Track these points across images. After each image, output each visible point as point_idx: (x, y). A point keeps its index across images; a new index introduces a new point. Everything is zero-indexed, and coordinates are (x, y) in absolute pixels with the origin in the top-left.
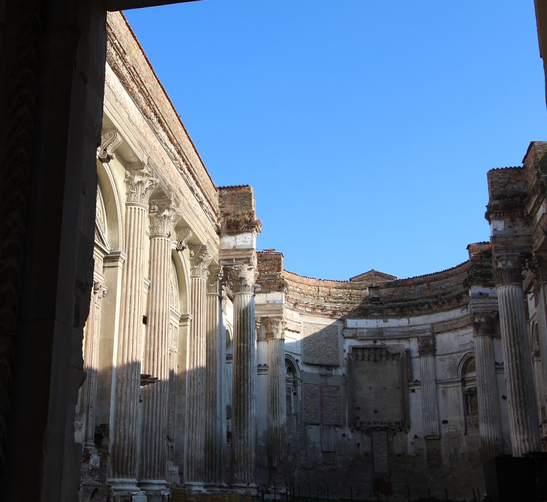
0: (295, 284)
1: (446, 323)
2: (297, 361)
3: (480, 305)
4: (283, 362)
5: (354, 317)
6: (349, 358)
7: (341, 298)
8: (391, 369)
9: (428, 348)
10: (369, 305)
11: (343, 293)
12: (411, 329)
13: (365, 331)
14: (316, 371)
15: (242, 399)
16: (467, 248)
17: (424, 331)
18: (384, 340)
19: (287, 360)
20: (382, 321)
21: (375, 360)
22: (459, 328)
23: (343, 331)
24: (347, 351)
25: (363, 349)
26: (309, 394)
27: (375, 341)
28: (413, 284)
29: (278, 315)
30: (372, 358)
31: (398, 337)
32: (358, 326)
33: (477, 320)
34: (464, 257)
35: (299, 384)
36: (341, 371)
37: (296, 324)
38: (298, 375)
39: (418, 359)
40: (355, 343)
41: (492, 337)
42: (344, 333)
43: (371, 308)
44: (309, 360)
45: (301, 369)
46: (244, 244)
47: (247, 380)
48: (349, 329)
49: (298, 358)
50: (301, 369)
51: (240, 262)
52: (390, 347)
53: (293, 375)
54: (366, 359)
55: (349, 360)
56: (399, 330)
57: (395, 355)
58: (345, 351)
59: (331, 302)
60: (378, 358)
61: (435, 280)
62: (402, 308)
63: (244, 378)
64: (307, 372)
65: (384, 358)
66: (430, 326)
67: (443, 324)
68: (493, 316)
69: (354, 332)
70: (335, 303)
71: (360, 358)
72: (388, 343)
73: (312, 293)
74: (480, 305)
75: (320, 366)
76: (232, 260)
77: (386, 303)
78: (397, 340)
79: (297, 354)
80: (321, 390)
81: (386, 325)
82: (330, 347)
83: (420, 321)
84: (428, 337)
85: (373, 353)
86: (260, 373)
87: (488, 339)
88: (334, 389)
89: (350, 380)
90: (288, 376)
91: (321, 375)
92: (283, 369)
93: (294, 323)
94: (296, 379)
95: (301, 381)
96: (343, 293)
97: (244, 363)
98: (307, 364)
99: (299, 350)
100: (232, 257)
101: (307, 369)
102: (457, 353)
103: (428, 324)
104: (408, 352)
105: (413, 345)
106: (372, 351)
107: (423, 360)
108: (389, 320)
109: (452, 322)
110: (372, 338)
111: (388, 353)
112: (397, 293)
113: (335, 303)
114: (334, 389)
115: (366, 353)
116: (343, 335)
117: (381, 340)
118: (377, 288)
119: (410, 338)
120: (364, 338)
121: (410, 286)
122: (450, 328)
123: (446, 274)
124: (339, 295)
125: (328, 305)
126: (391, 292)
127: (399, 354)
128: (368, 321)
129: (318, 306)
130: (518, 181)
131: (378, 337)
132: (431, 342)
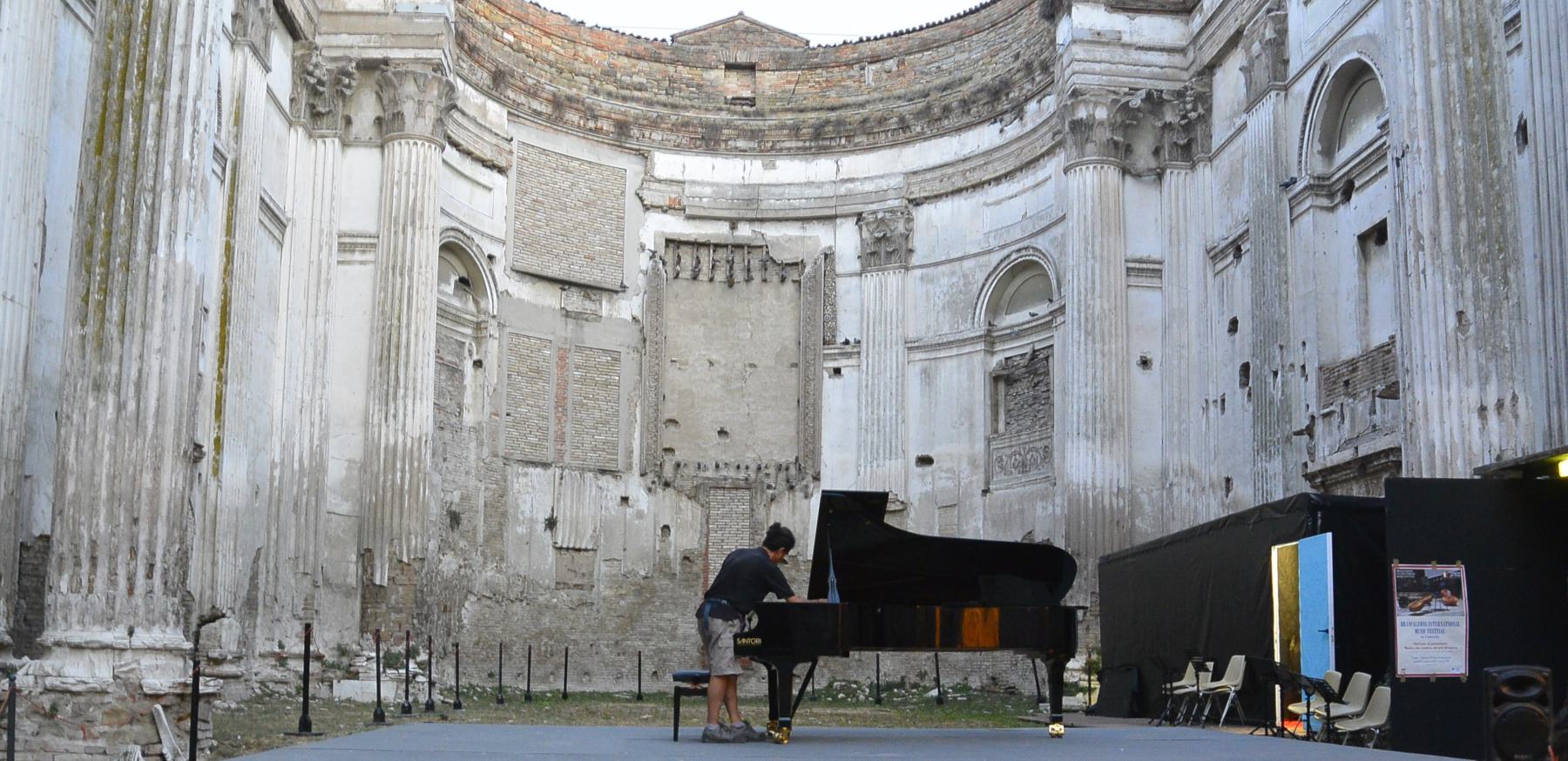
1: (950, 170)
2: (491, 257)
3: (1097, 67)
5: (678, 148)
6: (655, 268)
7: (640, 88)
8: (772, 312)
9: (887, 248)
10: (724, 116)
11: (649, 75)
12: (843, 190)
13: (708, 190)
14: (551, 298)
15: (126, 178)
17: (881, 195)
18: (762, 220)
20: (758, 163)
21: (730, 282)
23: (641, 188)
24: (650, 246)
25: (696, 245)
26: (524, 369)
27: (733, 227)
28: (859, 61)
29: (424, 54)
30: (721, 276)
31: (802, 214)
32: (687, 178)
33: (1082, 113)
35: (493, 329)
36: (629, 307)
37: (494, 140)
38: (491, 304)
39: (855, 280)
40: (678, 227)
41: (1125, 172)
42: (645, 194)
43: (728, 125)
45: (501, 288)
48: (660, 181)
49: (497, 251)
50: (501, 288)
52: (777, 242)
53: (476, 302)
54: (703, 277)
55: (653, 276)
56: (808, 192)
57: (788, 269)
58: (643, 248)
59: (609, 94)
60: (739, 276)
61: (925, 47)
62: (818, 132)
63: (143, 75)
64: (520, 301)
66: (900, 179)
67: (938, 173)
68: (1136, 102)
70: (625, 99)
72: (771, 232)
73: (551, 57)
74: (1097, 67)
75: (564, 284)
77: (773, 111)
78: (799, 224)
79: (492, 238)
80: (562, 358)
81: (770, 177)
82: (597, 232)
83: (873, 169)
84: (892, 211)
85: (725, 257)
86: (348, 257)
87: (1112, 174)
88: (603, 359)
89: (649, 335)
90: (456, 303)
91: (567, 314)
93: (487, 137)
94: (482, 317)
95: (501, 326)
96: (649, 75)
98: (524, 274)
99: (499, 227)
101: (524, 291)
102: (975, 255)
104: (828, 256)
105: (846, 241)
106: (722, 254)
107: (871, 281)
108: (778, 163)
109: (968, 165)
110: (726, 214)
111: (768, 262)
112: (808, 88)
113: (625, 99)
114: (603, 359)
115: (706, 257)
116: (641, 199)
117: (751, 220)
118: (751, 68)
121: (849, 65)
122: (960, 183)
123: (958, 27)
124: (636, 79)
125: (604, 104)
126: (789, 82)
127: (798, 265)
129: (569, 99)
131: (743, 214)
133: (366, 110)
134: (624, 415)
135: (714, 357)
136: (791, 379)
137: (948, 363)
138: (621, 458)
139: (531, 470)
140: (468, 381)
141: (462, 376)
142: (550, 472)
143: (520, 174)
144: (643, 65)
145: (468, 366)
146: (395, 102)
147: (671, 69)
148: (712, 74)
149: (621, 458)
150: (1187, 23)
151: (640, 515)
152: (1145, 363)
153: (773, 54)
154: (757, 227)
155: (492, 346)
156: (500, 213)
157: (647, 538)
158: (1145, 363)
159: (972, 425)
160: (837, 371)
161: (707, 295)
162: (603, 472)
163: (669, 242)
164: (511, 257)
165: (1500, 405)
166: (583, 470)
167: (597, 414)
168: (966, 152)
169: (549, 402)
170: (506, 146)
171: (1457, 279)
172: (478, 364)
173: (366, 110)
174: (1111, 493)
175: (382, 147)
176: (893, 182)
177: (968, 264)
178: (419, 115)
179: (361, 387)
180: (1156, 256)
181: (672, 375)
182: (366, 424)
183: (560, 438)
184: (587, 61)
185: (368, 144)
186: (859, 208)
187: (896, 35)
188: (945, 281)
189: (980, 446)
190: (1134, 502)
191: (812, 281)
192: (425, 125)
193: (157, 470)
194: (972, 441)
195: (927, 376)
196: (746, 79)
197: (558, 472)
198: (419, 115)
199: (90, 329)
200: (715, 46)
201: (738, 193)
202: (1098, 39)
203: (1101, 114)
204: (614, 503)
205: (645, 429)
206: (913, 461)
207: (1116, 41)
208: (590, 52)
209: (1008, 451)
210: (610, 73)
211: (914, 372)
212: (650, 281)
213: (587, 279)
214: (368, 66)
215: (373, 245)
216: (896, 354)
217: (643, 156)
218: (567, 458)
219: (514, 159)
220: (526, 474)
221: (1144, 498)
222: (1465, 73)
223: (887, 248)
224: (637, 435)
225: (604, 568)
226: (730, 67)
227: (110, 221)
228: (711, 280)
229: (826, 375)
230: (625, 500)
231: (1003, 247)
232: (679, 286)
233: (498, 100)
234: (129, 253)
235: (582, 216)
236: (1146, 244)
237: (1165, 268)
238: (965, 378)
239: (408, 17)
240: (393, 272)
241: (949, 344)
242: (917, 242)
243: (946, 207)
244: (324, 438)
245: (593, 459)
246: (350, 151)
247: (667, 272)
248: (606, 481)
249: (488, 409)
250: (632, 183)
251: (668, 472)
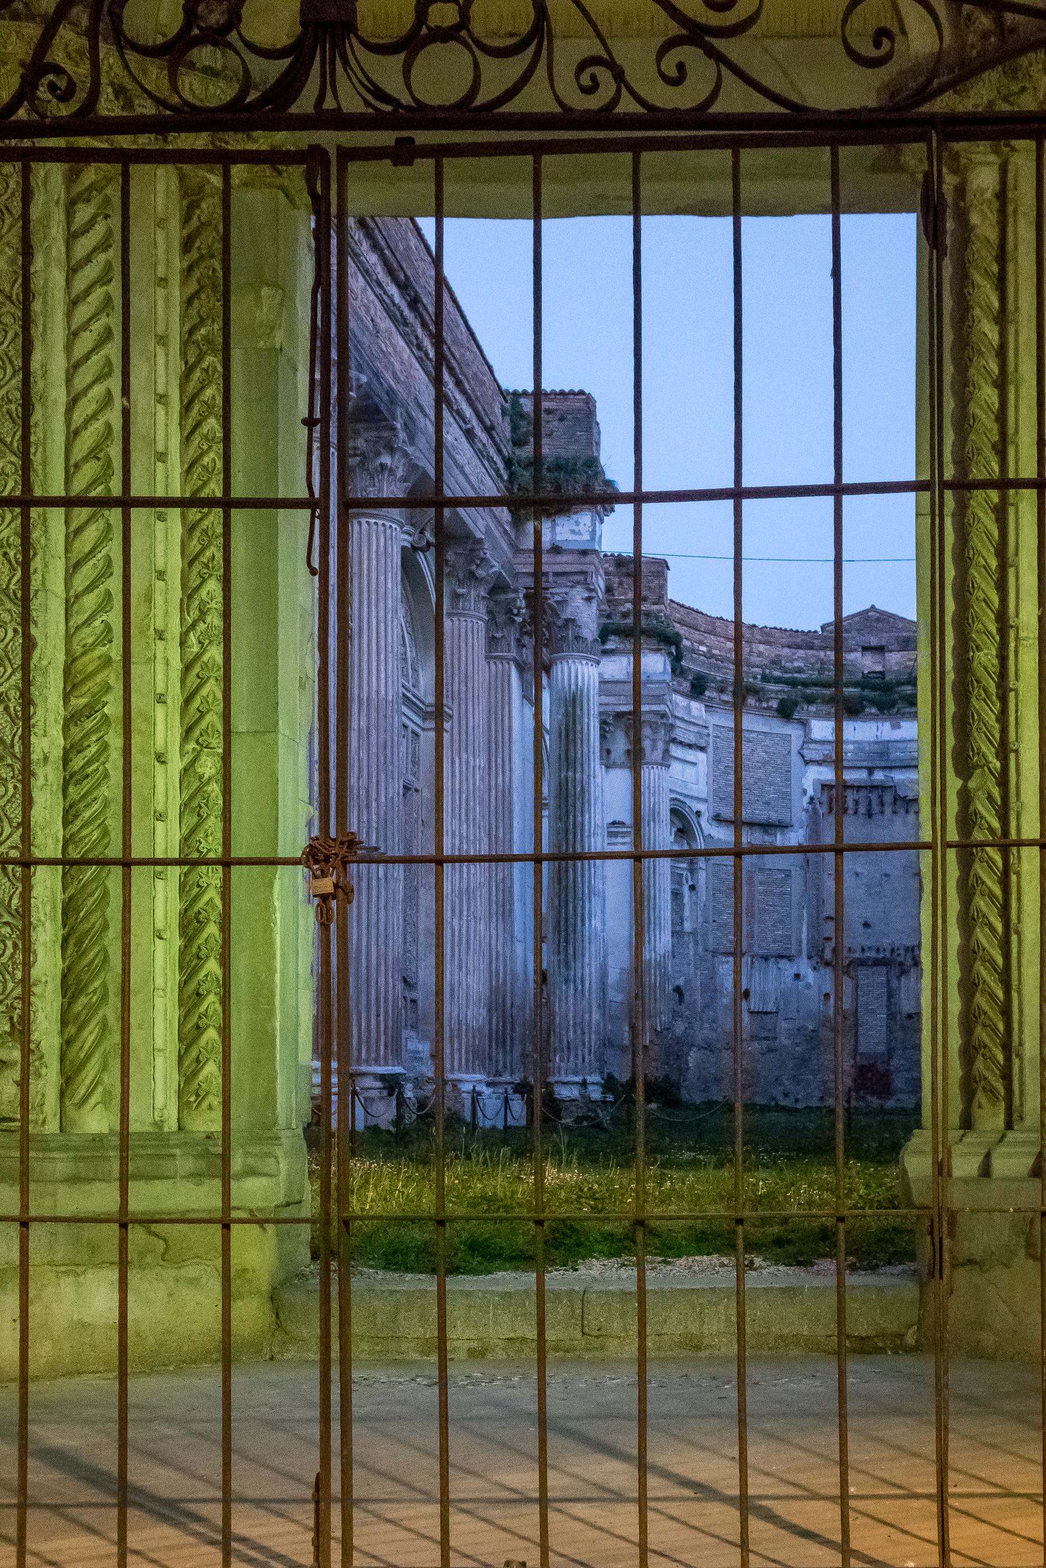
0: (697, 636)
2: (698, 814)
19: (674, 811)
23: (802, 748)
24: (810, 792)
27: (871, 770)
29: (655, 708)
42: (805, 752)
45: (706, 833)
48: (816, 742)
49: (701, 807)
50: (706, 833)
58: (805, 792)
79: (699, 799)
86: (613, 840)
93: (692, 728)
96: (805, 659)
97: (574, 816)
99: (702, 789)
118: (881, 649)
124: (796, 664)
133: (620, 745)
134: (795, 913)
135: (859, 870)
140: (686, 900)
141: (682, 897)
143: (716, 748)
144: (801, 653)
145: (686, 888)
147: (822, 654)
151: (808, 986)
155: (702, 875)
157: (814, 1002)
162: (781, 957)
163: (823, 786)
166: (766, 958)
167: (776, 915)
170: (705, 731)
172: (692, 888)
178: (654, 748)
184: (760, 654)
185: (621, 766)
196: (878, 657)
200: (854, 633)
201: (875, 747)
204: (789, 980)
208: (762, 647)
210: (776, 662)
212: (811, 817)
218: (756, 949)
219: (711, 739)
224: (804, 929)
225: (784, 1025)
226: (865, 649)
228: (856, 812)
230: (797, 976)
244: (605, 956)
245: (774, 948)
248: (783, 964)
249: (700, 920)
251: (828, 955)
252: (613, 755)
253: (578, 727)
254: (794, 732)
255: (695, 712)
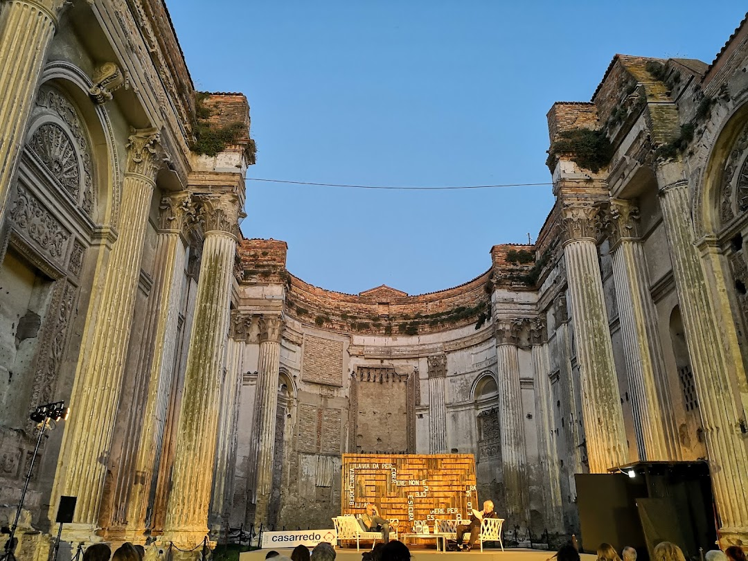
1: (459, 341)
3: (505, 311)
4: (276, 370)
8: (397, 394)
12: (421, 348)
14: (316, 390)
16: (491, 252)
17: (435, 350)
20: (390, 338)
21: (381, 382)
22: (473, 346)
27: (382, 362)
31: (407, 356)
33: (501, 327)
34: (486, 264)
36: (345, 392)
37: (297, 334)
39: (427, 381)
40: (362, 362)
42: (350, 351)
44: (309, 378)
45: (298, 388)
46: (227, 166)
47: (211, 358)
48: (355, 346)
49: (297, 374)
50: (298, 388)
51: (218, 190)
54: (371, 381)
56: (409, 349)
58: (349, 370)
60: (384, 380)
61: (449, 296)
63: (205, 354)
65: (391, 380)
67: (455, 342)
68: (520, 323)
69: (360, 349)
71: (365, 379)
72: (396, 363)
73: (317, 303)
74: (505, 311)
75: (322, 385)
76: (206, 187)
78: (405, 360)
81: (395, 343)
83: (431, 340)
86: (247, 383)
87: (513, 348)
88: (335, 412)
91: (322, 396)
92: (273, 379)
93: (294, 333)
95: (298, 402)
96: (351, 307)
97: (208, 332)
99: (298, 366)
100: (208, 183)
103: (439, 343)
104: (417, 372)
105: (423, 366)
106: (378, 371)
107: (433, 381)
109: (465, 340)
110: (379, 357)
112: (409, 310)
114: (335, 412)
118: (387, 304)
119: (419, 358)
120: (371, 357)
123: (460, 290)
124: (347, 309)
128: (376, 338)
130: (589, 119)
131: (385, 357)
132: (442, 362)
133: (254, 331)
134: (342, 434)
135: (376, 411)
136: (404, 418)
137: (462, 412)
138: (341, 450)
139: (307, 456)
141: (283, 421)
142: (314, 456)
143: (306, 346)
144: (349, 304)
145: (286, 416)
146: (264, 328)
147: (359, 305)
148: (374, 307)
149: (341, 450)
150: (537, 294)
152: (530, 416)
153: (395, 299)
154: (391, 362)
156: (298, 362)
158: (530, 416)
159: (471, 437)
160: (421, 416)
161: (372, 387)
162: (335, 456)
164: (302, 376)
165: (614, 448)
168: (465, 335)
169: (314, 430)
170: (301, 336)
171: (597, 408)
172: (289, 416)
173: (254, 331)
174: (519, 466)
175: (260, 344)
176: (439, 345)
177: (467, 376)
178: (273, 333)
179: (250, 430)
180: (531, 377)
181: (360, 417)
182: (251, 443)
183: (319, 444)
186: (427, 354)
187: (438, 292)
188: (459, 382)
189: (475, 445)
190: (529, 469)
191: (412, 382)
192: (275, 337)
193: (204, 474)
194: (472, 443)
195: (455, 418)
196: (386, 308)
197: (317, 457)
198: (273, 333)
199: (187, 431)
200: (374, 296)
202: (505, 301)
203: (508, 327)
205: (350, 439)
206: (450, 451)
207: (512, 302)
208: (331, 300)
209: (485, 447)
210: (337, 308)
211: (449, 416)
212: (352, 383)
213: (329, 382)
214: (255, 316)
215: (256, 379)
216: (442, 410)
217: (350, 337)
220: (306, 458)
221: (532, 467)
222: (595, 343)
223: (437, 369)
224: (347, 441)
226: (380, 304)
227: (194, 399)
228: (374, 381)
229: (417, 417)
231: (479, 370)
232: (362, 384)
233: (298, 320)
234: (200, 409)
235: (327, 360)
236: (527, 373)
237: (534, 381)
238: (468, 420)
239: (270, 300)
240: (262, 389)
241: (461, 406)
242: (448, 367)
243: (458, 354)
246: (248, 345)
247: (358, 379)
248: (335, 459)
250: (345, 347)
252: (250, 338)
253: (218, 275)
254: (346, 341)
255: (296, 326)
